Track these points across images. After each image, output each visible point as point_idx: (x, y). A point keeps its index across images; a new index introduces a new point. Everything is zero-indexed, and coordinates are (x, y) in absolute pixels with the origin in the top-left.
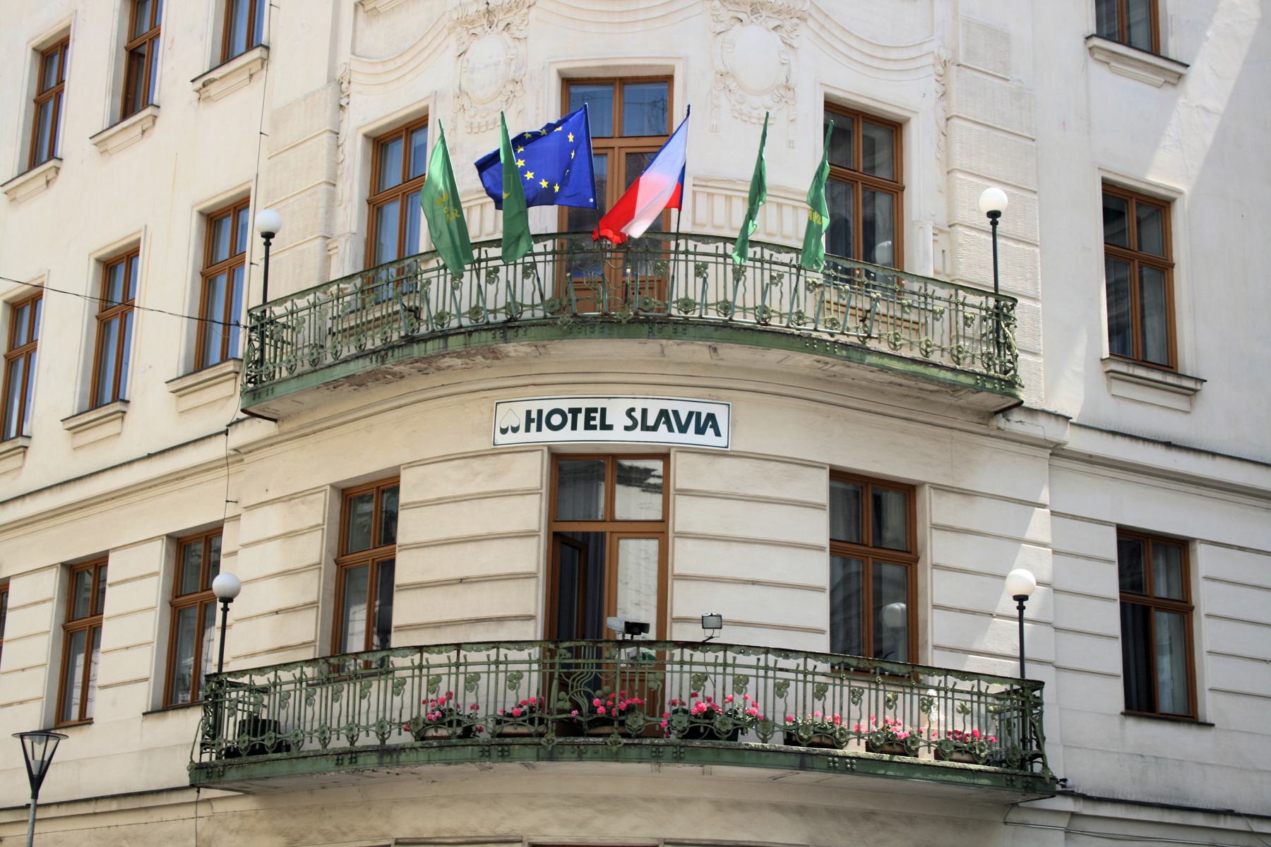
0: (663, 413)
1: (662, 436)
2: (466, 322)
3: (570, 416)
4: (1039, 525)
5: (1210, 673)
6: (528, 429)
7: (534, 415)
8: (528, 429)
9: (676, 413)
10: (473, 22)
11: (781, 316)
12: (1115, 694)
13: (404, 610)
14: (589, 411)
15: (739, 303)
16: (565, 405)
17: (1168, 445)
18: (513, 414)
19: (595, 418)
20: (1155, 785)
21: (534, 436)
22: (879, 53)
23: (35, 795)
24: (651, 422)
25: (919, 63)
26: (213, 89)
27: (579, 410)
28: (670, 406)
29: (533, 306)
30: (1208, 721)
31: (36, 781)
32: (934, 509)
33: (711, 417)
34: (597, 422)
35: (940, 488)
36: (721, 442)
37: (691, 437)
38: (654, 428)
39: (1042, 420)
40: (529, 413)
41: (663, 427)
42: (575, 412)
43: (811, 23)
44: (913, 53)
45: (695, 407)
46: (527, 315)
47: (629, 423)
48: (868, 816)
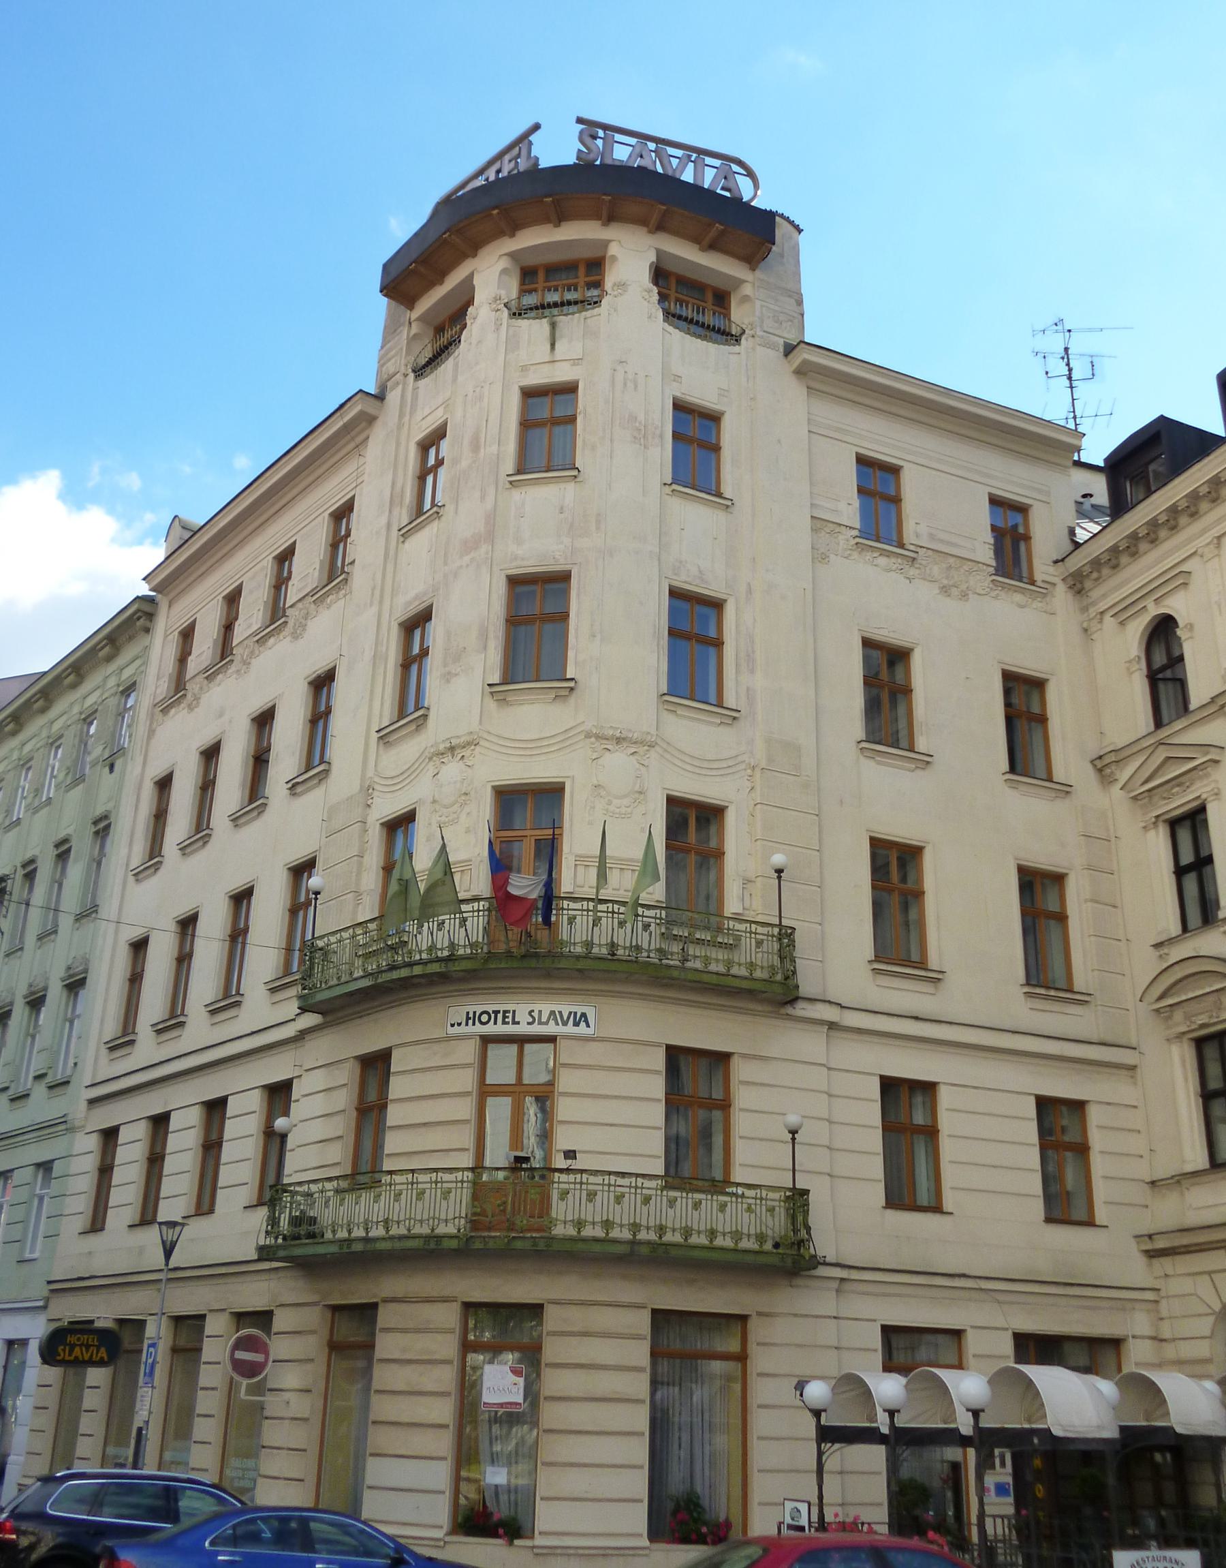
0: (552, 1013)
2: (424, 956)
3: (493, 1016)
6: (467, 1024)
7: (471, 1015)
8: (467, 1024)
9: (560, 1013)
10: (442, 754)
11: (625, 948)
12: (878, 1193)
13: (393, 1143)
14: (505, 1012)
15: (596, 941)
16: (490, 1009)
17: (916, 1018)
21: (471, 1029)
22: (706, 765)
23: (167, 1264)
24: (544, 1019)
26: (299, 789)
27: (499, 1012)
28: (556, 1008)
29: (465, 946)
30: (949, 1211)
31: (168, 1253)
32: (740, 1070)
33: (584, 1015)
34: (510, 1020)
35: (744, 1056)
36: (590, 1031)
37: (570, 1029)
38: (547, 1023)
40: (468, 1013)
41: (552, 1022)
42: (496, 1012)
43: (657, 748)
44: (730, 763)
45: (573, 1009)
46: (461, 952)
47: (531, 1020)
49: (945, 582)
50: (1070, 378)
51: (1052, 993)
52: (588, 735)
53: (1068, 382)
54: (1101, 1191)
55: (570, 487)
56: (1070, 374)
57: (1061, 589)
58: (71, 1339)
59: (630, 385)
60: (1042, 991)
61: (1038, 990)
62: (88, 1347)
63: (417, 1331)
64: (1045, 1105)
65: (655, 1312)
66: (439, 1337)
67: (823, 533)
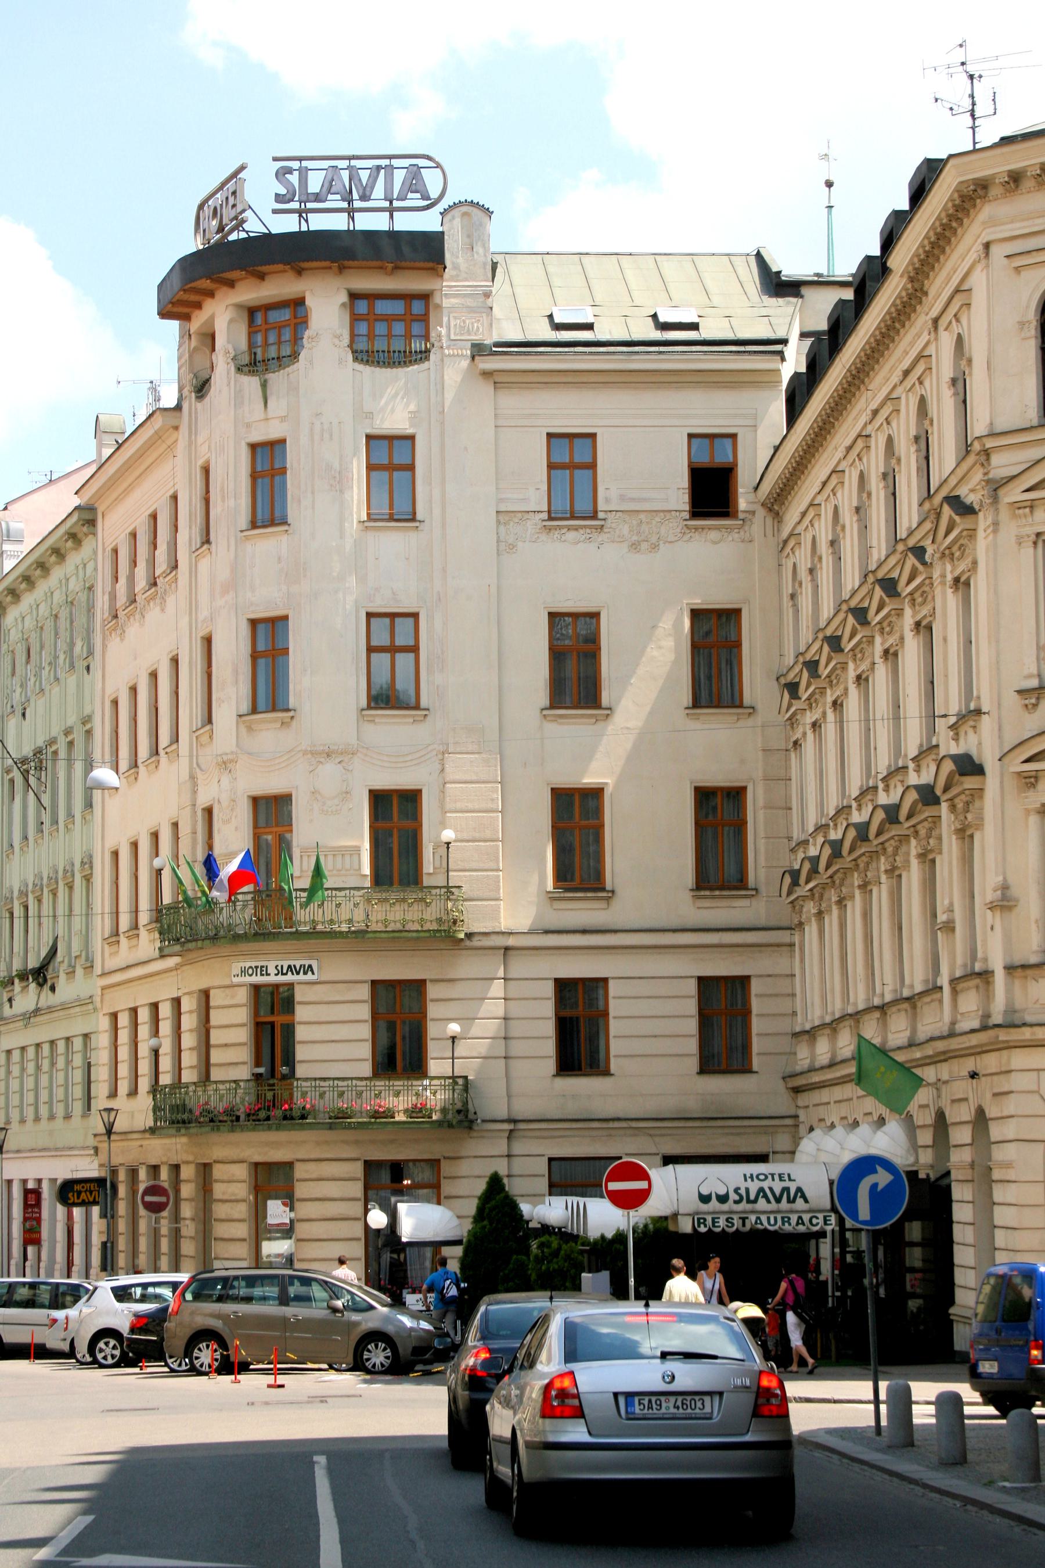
0: (289, 967)
1: (290, 978)
4: (497, 988)
5: (616, 1047)
12: (551, 1065)
14: (262, 967)
16: (253, 964)
18: (236, 968)
19: (263, 971)
20: (572, 1109)
22: (401, 759)
25: (428, 756)
28: (292, 963)
32: (432, 991)
33: (310, 966)
35: (432, 981)
36: (315, 977)
37: (301, 977)
38: (286, 974)
39: (493, 937)
41: (290, 973)
42: (257, 967)
43: (359, 754)
44: (422, 753)
45: (303, 962)
48: (392, 1141)
49: (635, 538)
50: (973, 116)
51: (717, 893)
52: (305, 753)
53: (970, 119)
54: (757, 1045)
55: (285, 538)
56: (973, 110)
57: (761, 512)
58: (77, 1187)
59: (326, 436)
60: (707, 893)
61: (702, 893)
62: (91, 1192)
63: (229, 1182)
64: (705, 983)
65: (366, 1162)
66: (239, 1185)
67: (512, 524)
